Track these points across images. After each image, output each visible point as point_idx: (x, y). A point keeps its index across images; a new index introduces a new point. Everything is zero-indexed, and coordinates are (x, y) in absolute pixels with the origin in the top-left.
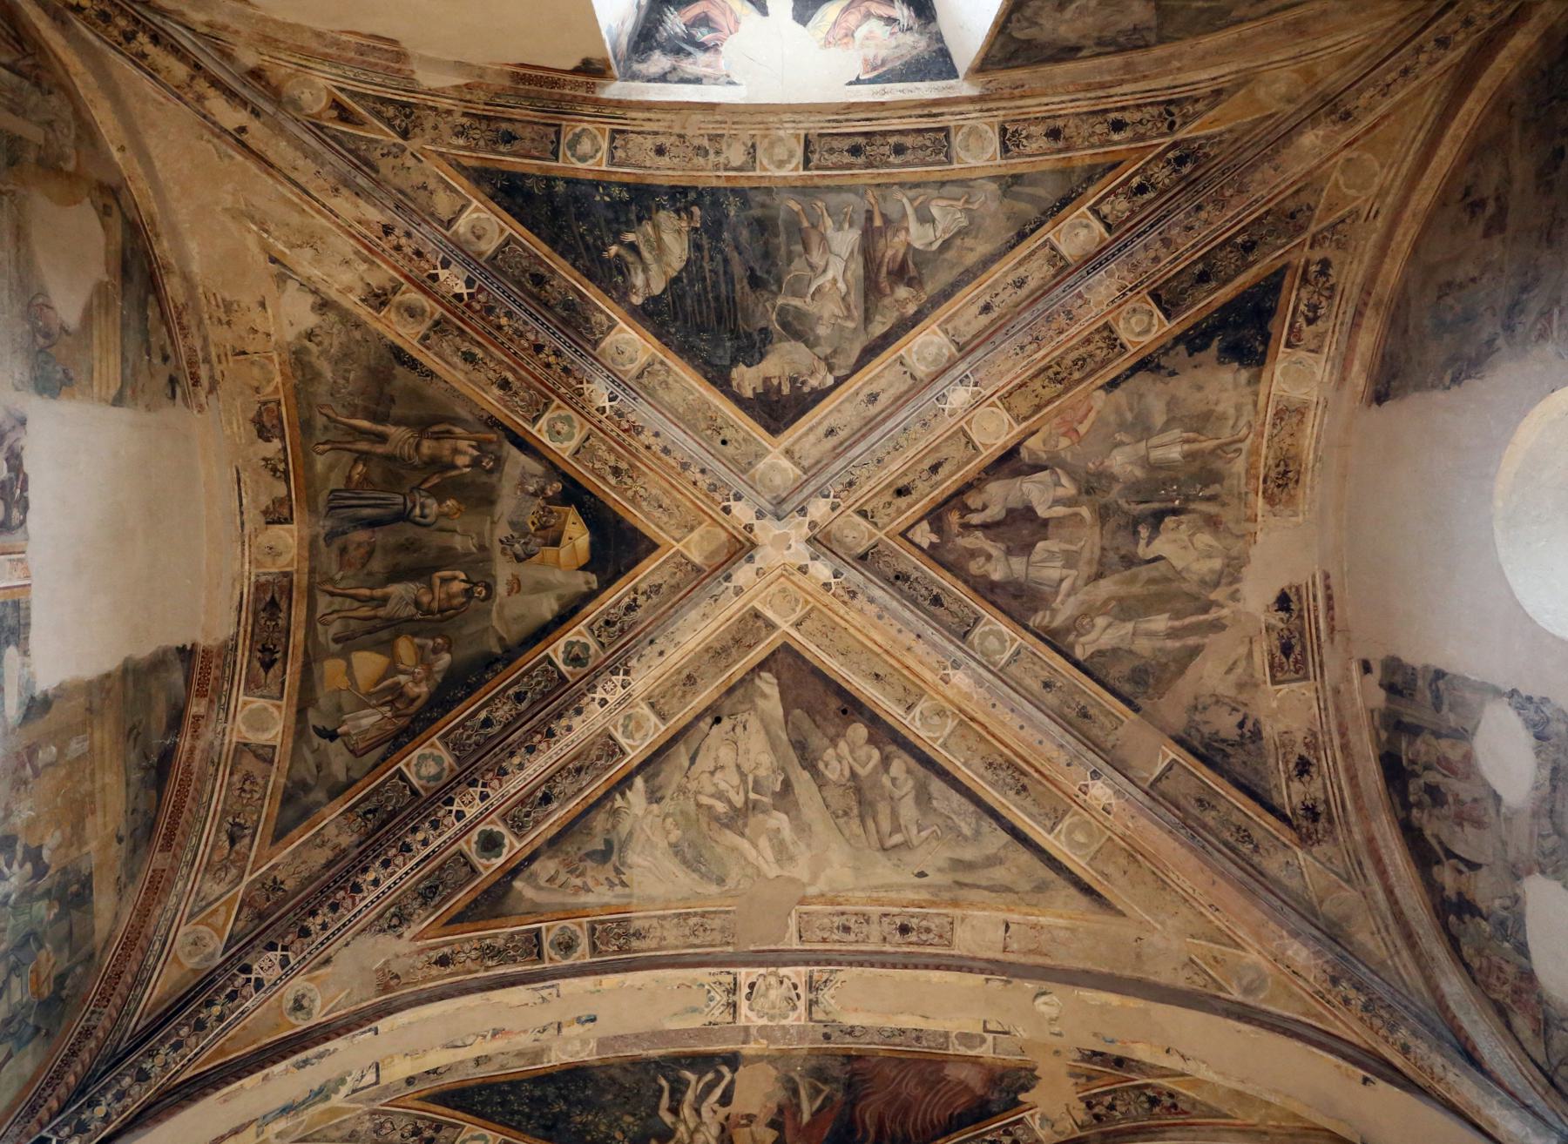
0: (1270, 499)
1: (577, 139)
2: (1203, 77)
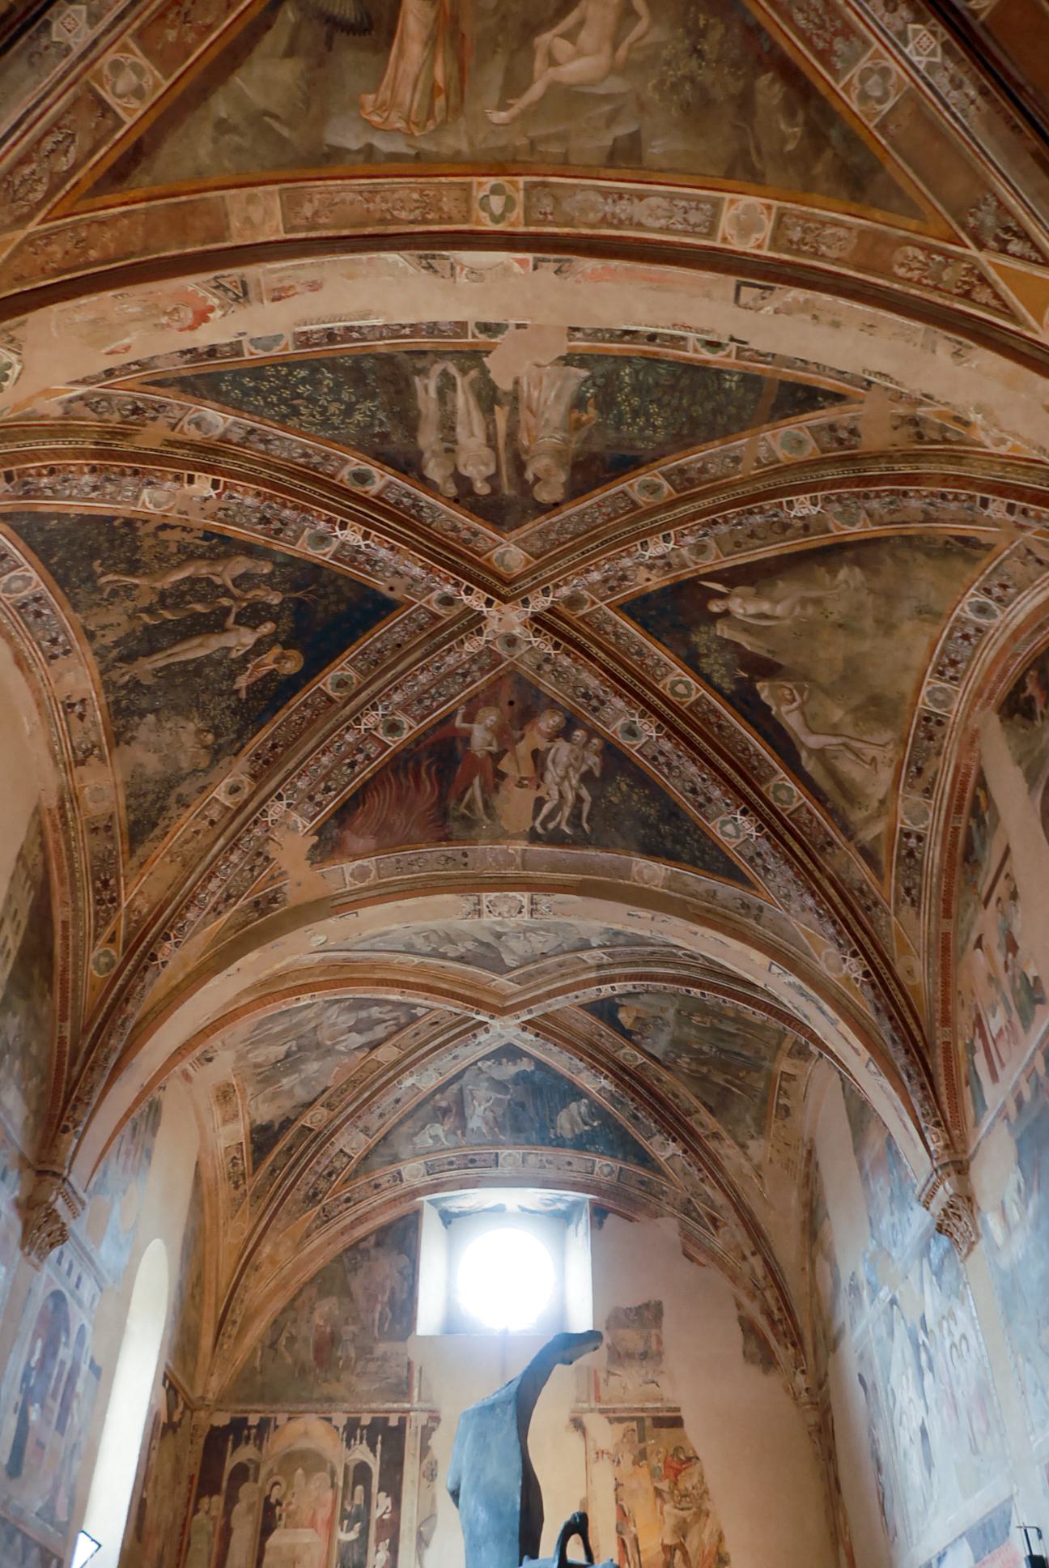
0: (230, 1085)
1: (609, 1174)
2: (317, 1241)
